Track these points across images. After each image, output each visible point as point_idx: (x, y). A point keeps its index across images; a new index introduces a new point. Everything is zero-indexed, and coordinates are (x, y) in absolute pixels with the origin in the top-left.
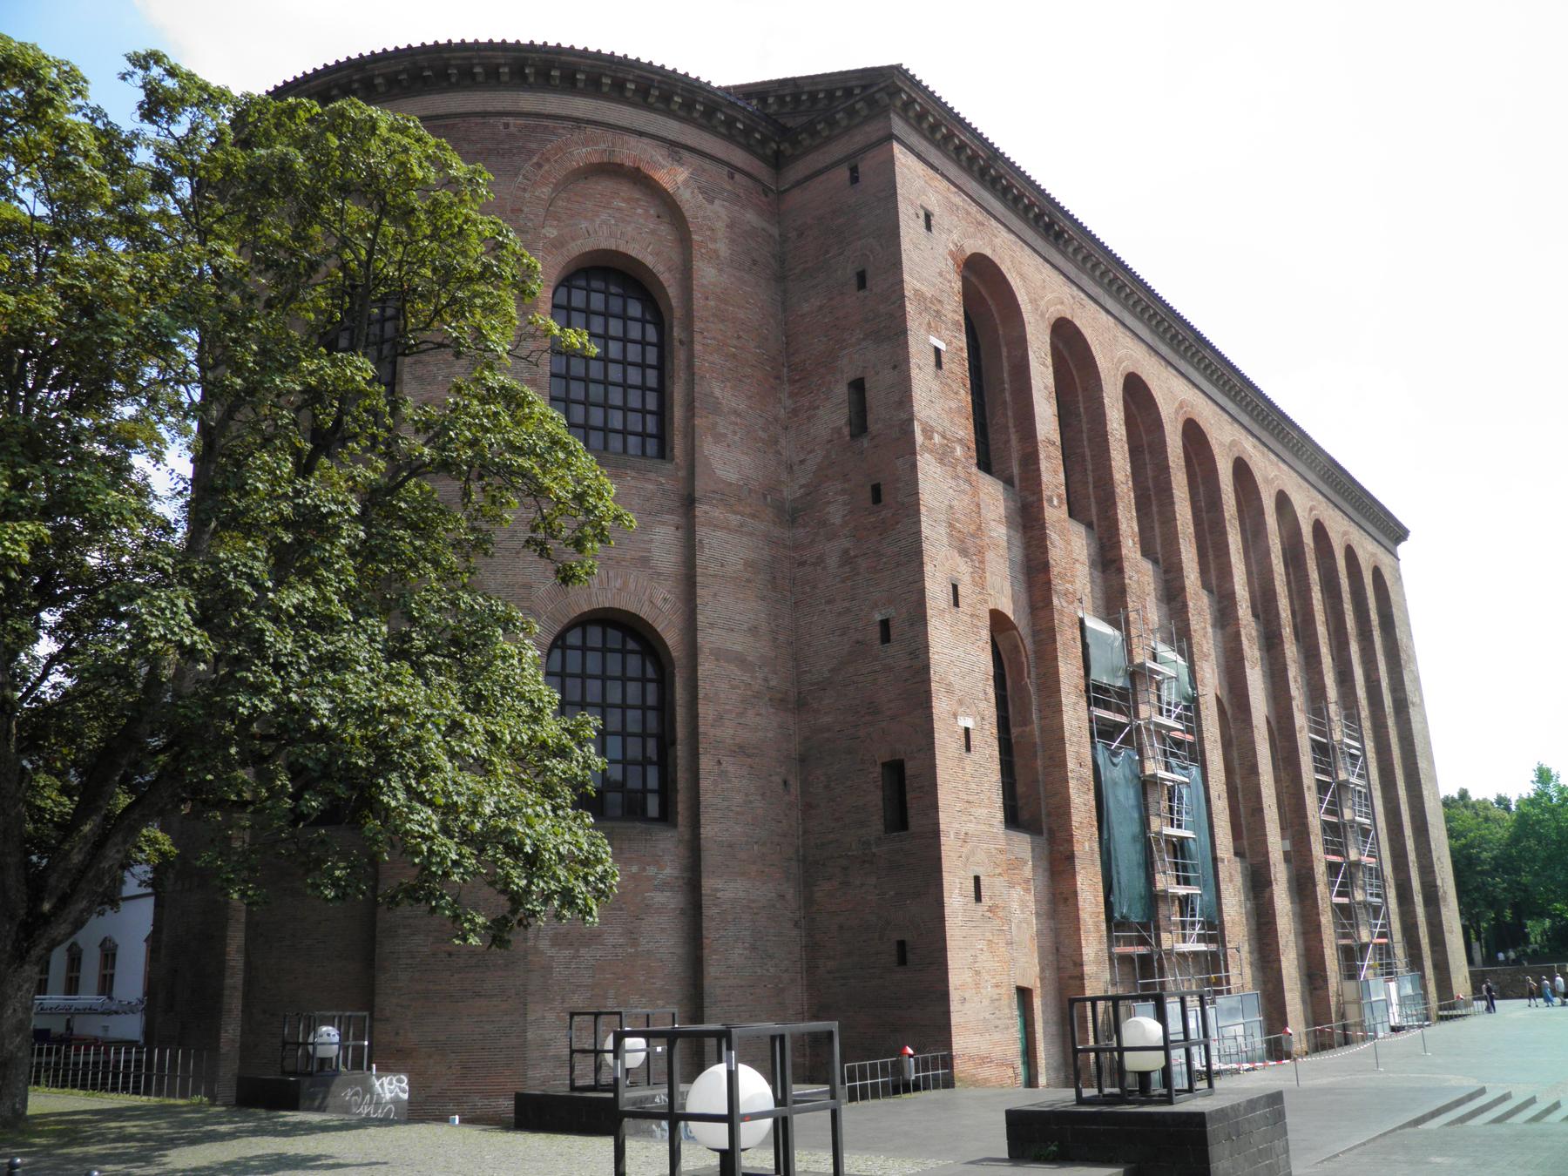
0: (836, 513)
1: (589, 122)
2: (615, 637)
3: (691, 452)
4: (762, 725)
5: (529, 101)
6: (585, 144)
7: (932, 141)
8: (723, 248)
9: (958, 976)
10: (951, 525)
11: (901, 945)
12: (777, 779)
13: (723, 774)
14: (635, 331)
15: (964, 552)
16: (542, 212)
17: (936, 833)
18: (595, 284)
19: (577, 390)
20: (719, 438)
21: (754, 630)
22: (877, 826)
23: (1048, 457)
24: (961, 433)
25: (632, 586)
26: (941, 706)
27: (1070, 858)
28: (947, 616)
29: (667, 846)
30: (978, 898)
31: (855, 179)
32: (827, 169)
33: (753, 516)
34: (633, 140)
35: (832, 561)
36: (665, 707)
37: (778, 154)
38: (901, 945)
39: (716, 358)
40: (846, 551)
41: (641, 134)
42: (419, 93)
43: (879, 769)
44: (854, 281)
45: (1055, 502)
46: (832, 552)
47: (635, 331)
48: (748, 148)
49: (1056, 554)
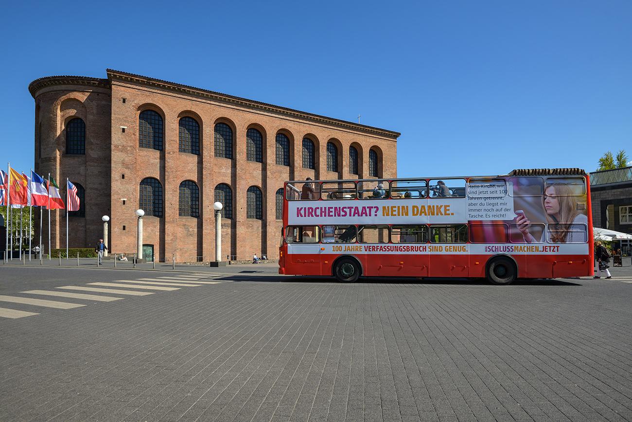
1: (65, 90)
5: (55, 88)
8: (95, 111)
13: (91, 209)
15: (128, 168)
20: (92, 149)
21: (100, 184)
23: (170, 144)
25: (76, 178)
29: (82, 219)
39: (92, 134)
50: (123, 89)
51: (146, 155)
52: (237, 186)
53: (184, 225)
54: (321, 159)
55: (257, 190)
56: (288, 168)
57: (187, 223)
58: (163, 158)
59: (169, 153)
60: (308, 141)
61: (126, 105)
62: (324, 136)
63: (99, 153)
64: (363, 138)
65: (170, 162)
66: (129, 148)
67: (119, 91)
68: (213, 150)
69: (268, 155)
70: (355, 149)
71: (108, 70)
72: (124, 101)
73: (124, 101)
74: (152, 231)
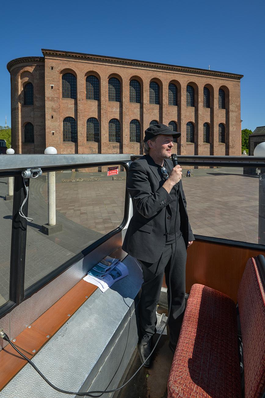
10: (52, 109)
23: (80, 94)
45: (81, 100)
50: (51, 60)
51: (66, 103)
52: (123, 120)
53: (90, 147)
54: (182, 98)
55: (137, 122)
56: (158, 106)
57: (91, 146)
58: (76, 104)
59: (80, 100)
60: (173, 86)
61: (54, 69)
62: (185, 81)
64: (214, 80)
65: (80, 106)
66: (55, 99)
67: (49, 62)
68: (108, 97)
69: (144, 97)
70: (208, 89)
71: (42, 50)
72: (52, 69)
73: (52, 69)
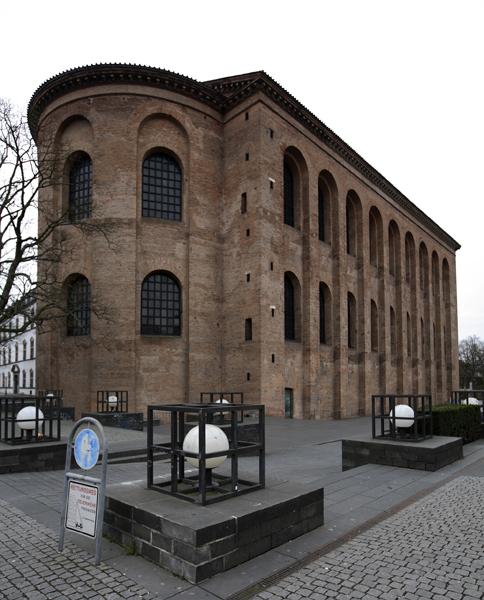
0: (236, 239)
2: (164, 279)
3: (189, 219)
4: (211, 306)
5: (132, 89)
6: (152, 105)
7: (276, 102)
8: (201, 146)
9: (264, 384)
10: (272, 243)
11: (248, 374)
12: (215, 323)
14: (172, 176)
15: (276, 252)
16: (136, 132)
17: (260, 341)
18: (158, 159)
19: (152, 198)
20: (198, 214)
21: (208, 277)
22: (244, 339)
24: (279, 212)
26: (264, 302)
27: (309, 350)
28: (268, 274)
30: (273, 361)
31: (247, 118)
32: (240, 113)
33: (211, 240)
34: (168, 104)
35: (234, 255)
36: (180, 301)
37: (223, 108)
38: (248, 374)
40: (238, 252)
41: (172, 102)
42: (94, 85)
43: (244, 322)
44: (245, 157)
46: (235, 251)
47: (172, 176)
48: (212, 107)
49: (314, 252)
63: (206, 221)
66: (277, 218)
74: (292, 364)
